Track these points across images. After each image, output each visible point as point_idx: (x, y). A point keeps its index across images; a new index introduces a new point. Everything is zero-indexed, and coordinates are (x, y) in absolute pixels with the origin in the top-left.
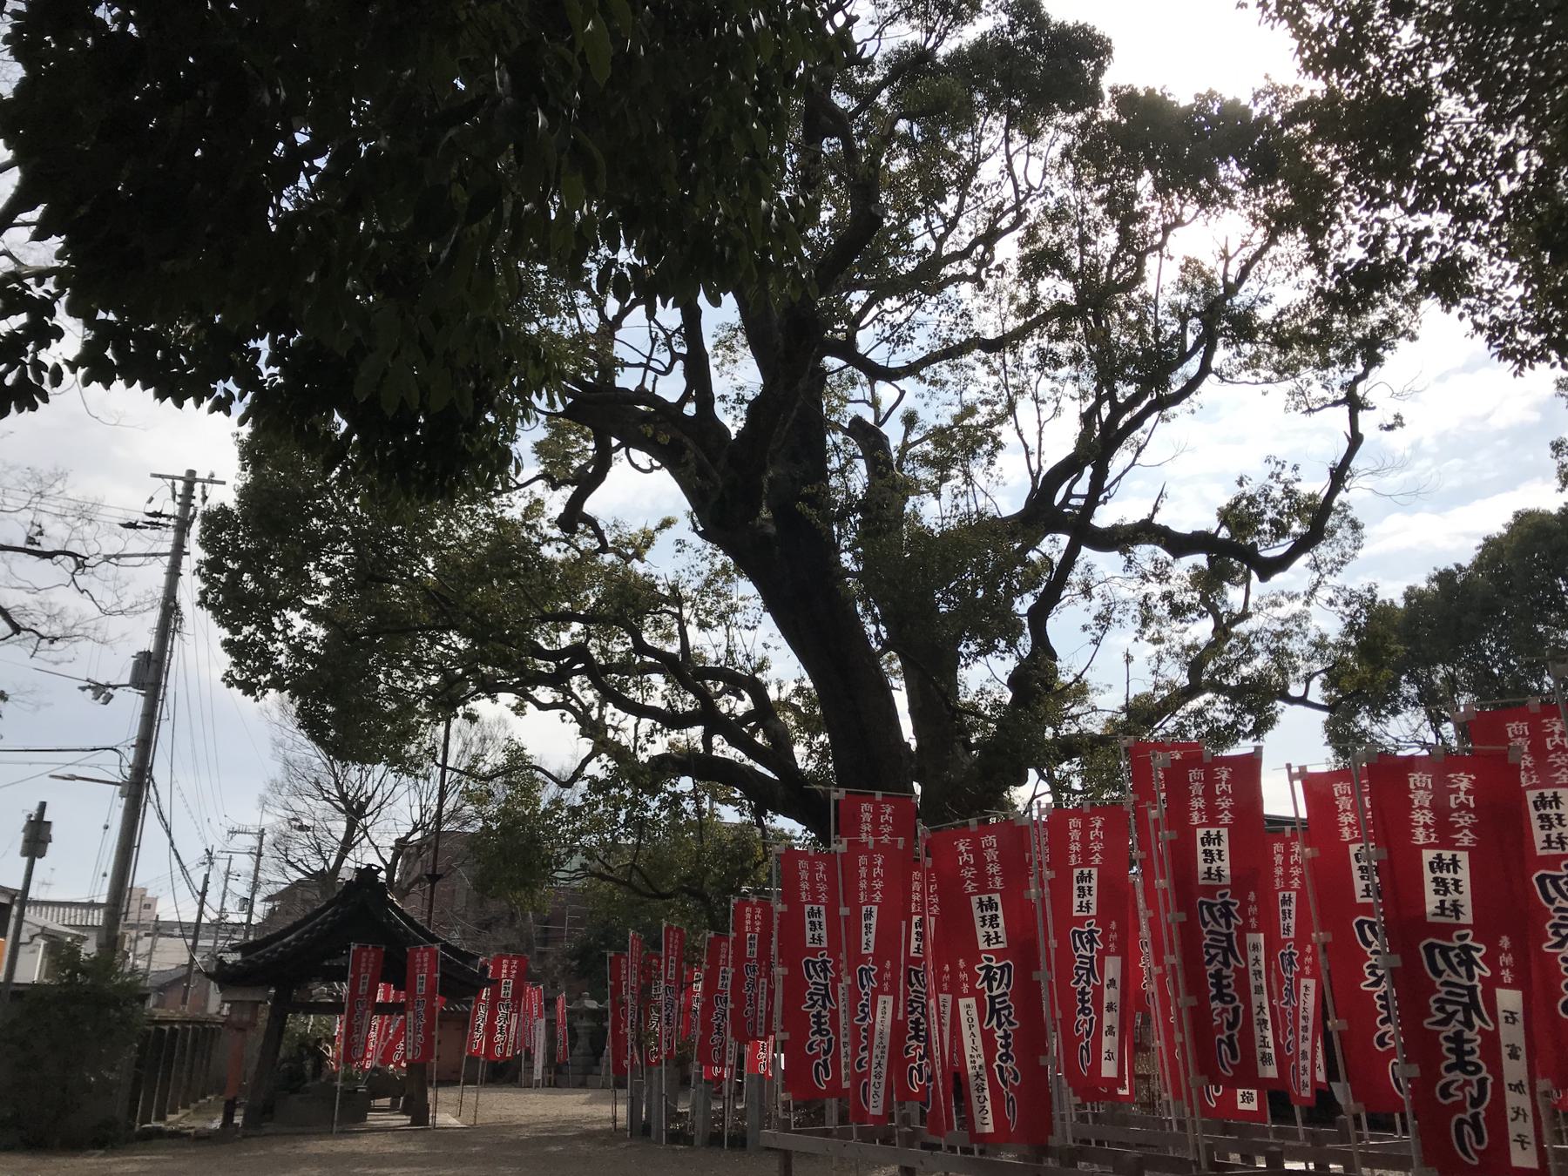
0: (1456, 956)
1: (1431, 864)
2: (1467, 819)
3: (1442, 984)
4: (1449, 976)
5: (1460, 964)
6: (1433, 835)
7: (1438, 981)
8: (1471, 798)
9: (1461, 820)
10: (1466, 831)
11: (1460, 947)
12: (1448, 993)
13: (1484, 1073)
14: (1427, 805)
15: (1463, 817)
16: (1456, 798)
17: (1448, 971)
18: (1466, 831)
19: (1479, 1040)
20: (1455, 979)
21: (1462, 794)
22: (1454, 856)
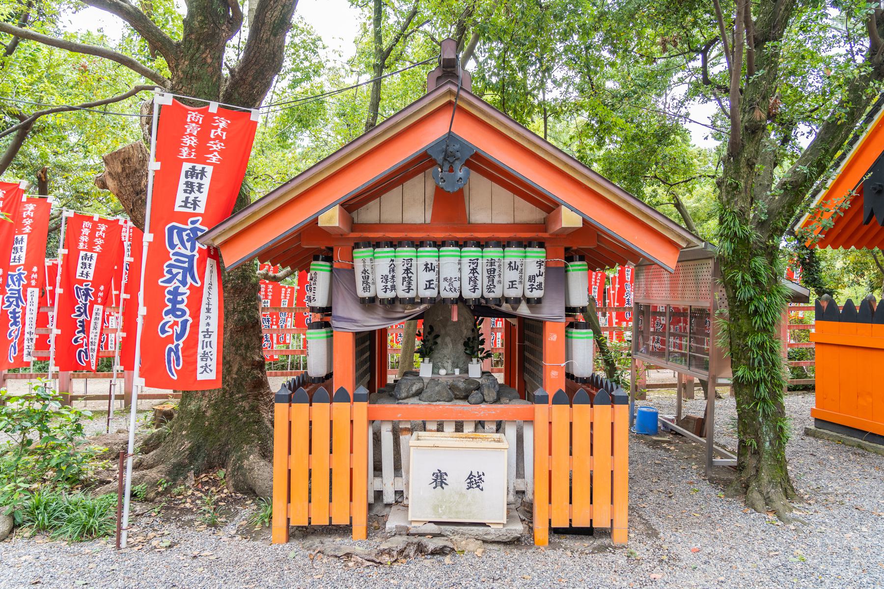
0: (187, 235)
1: (187, 172)
2: (218, 145)
3: (175, 254)
4: (179, 249)
5: (188, 241)
6: (193, 154)
7: (172, 252)
8: (225, 133)
9: (214, 146)
10: (216, 153)
11: (191, 229)
12: (176, 260)
13: (187, 317)
14: (195, 134)
15: (216, 144)
16: (215, 132)
17: (180, 245)
18: (216, 153)
19: (188, 292)
20: (183, 251)
21: (219, 131)
22: (203, 168)
